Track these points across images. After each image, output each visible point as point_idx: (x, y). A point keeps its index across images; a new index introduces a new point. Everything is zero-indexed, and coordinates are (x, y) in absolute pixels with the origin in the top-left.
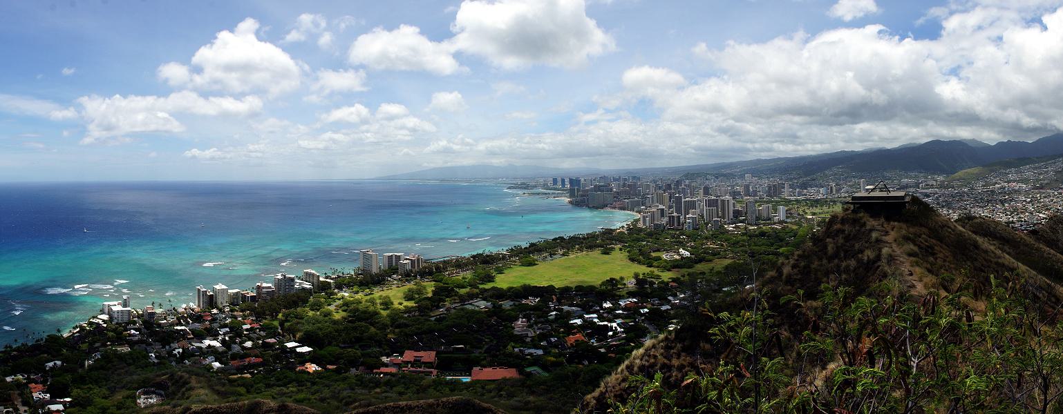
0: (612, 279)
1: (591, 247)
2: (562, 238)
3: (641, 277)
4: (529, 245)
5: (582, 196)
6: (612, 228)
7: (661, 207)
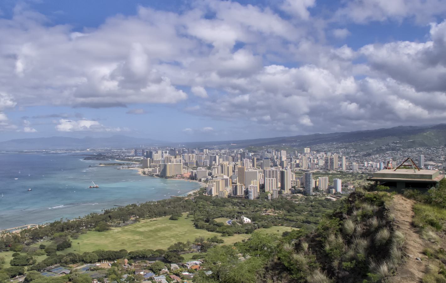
0: (180, 243)
1: (160, 214)
2: (134, 206)
3: (205, 241)
4: (104, 211)
5: (154, 167)
6: (181, 196)
7: (225, 177)
